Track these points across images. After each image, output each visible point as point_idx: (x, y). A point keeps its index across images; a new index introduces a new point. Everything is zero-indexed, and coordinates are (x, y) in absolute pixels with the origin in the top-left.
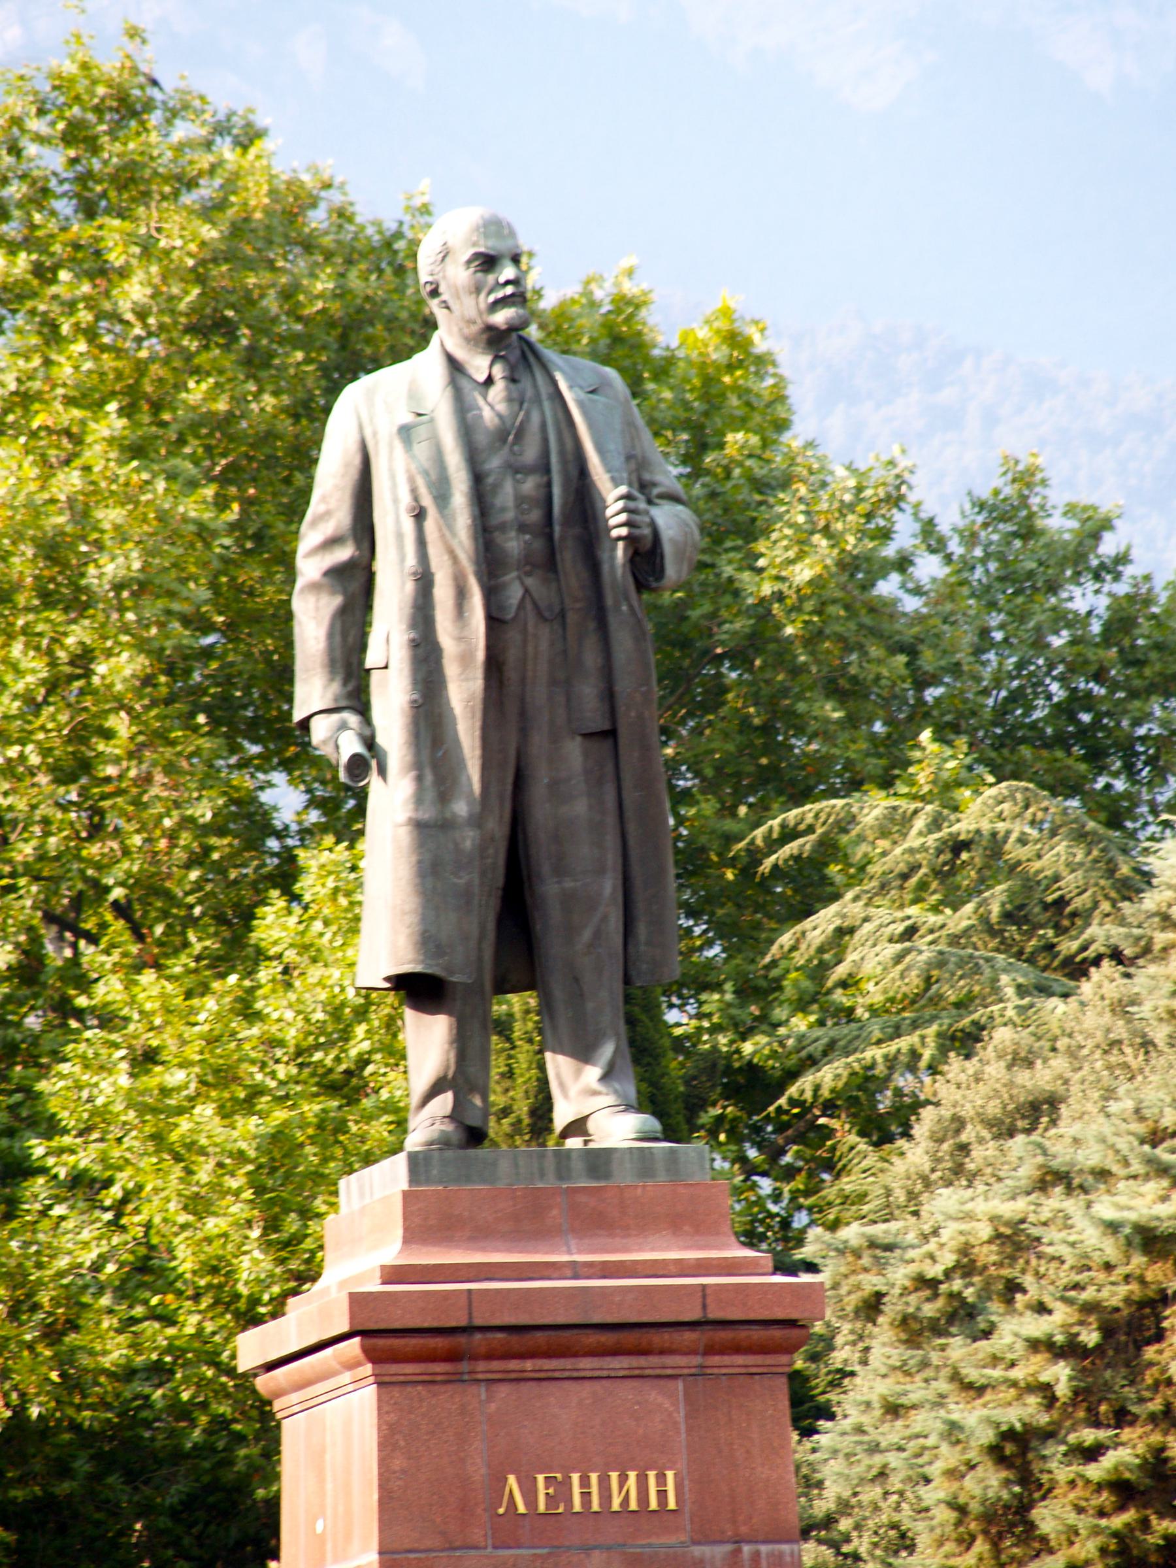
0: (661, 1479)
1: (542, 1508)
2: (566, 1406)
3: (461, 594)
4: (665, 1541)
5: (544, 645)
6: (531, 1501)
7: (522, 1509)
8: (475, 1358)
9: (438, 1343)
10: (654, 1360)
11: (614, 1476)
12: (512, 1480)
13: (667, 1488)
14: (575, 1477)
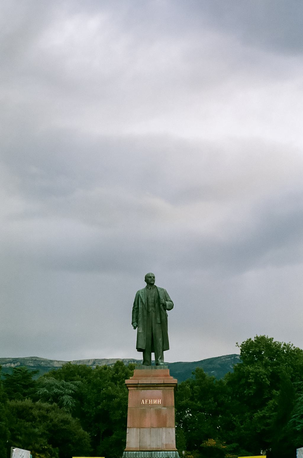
0: (159, 400)
1: (146, 403)
5: (154, 315)
6: (145, 402)
7: (144, 404)
10: (159, 388)
12: (143, 400)
14: (150, 400)
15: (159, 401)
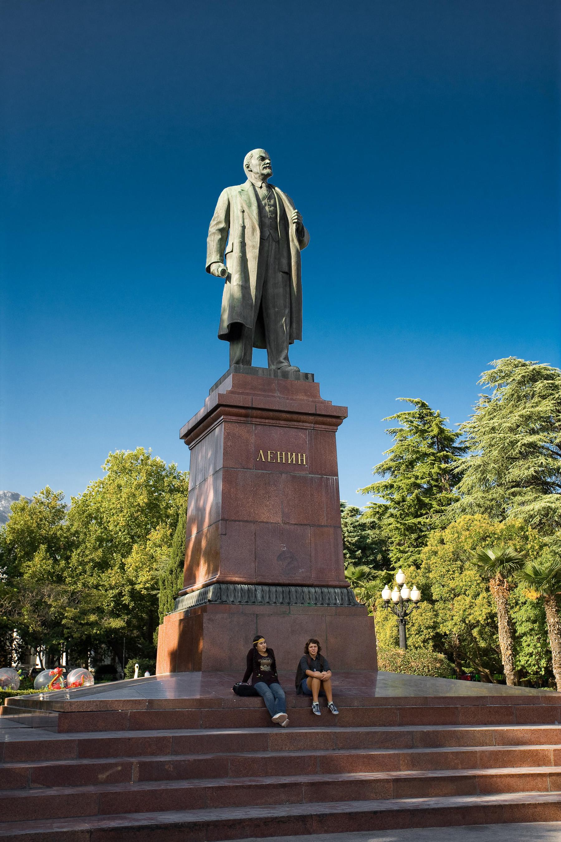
0: (302, 456)
1: (269, 460)
2: (277, 434)
3: (254, 230)
4: (303, 474)
5: (274, 248)
7: (264, 460)
8: (252, 417)
9: (243, 411)
11: (289, 454)
12: (261, 451)
13: (303, 459)
14: (279, 453)
15: (303, 459)
